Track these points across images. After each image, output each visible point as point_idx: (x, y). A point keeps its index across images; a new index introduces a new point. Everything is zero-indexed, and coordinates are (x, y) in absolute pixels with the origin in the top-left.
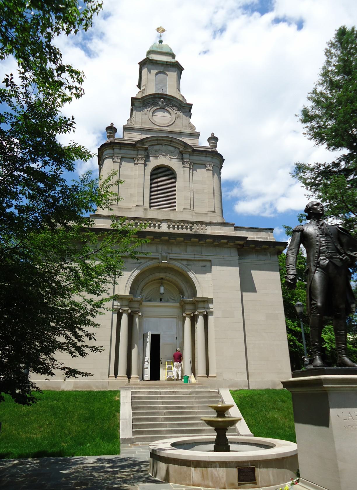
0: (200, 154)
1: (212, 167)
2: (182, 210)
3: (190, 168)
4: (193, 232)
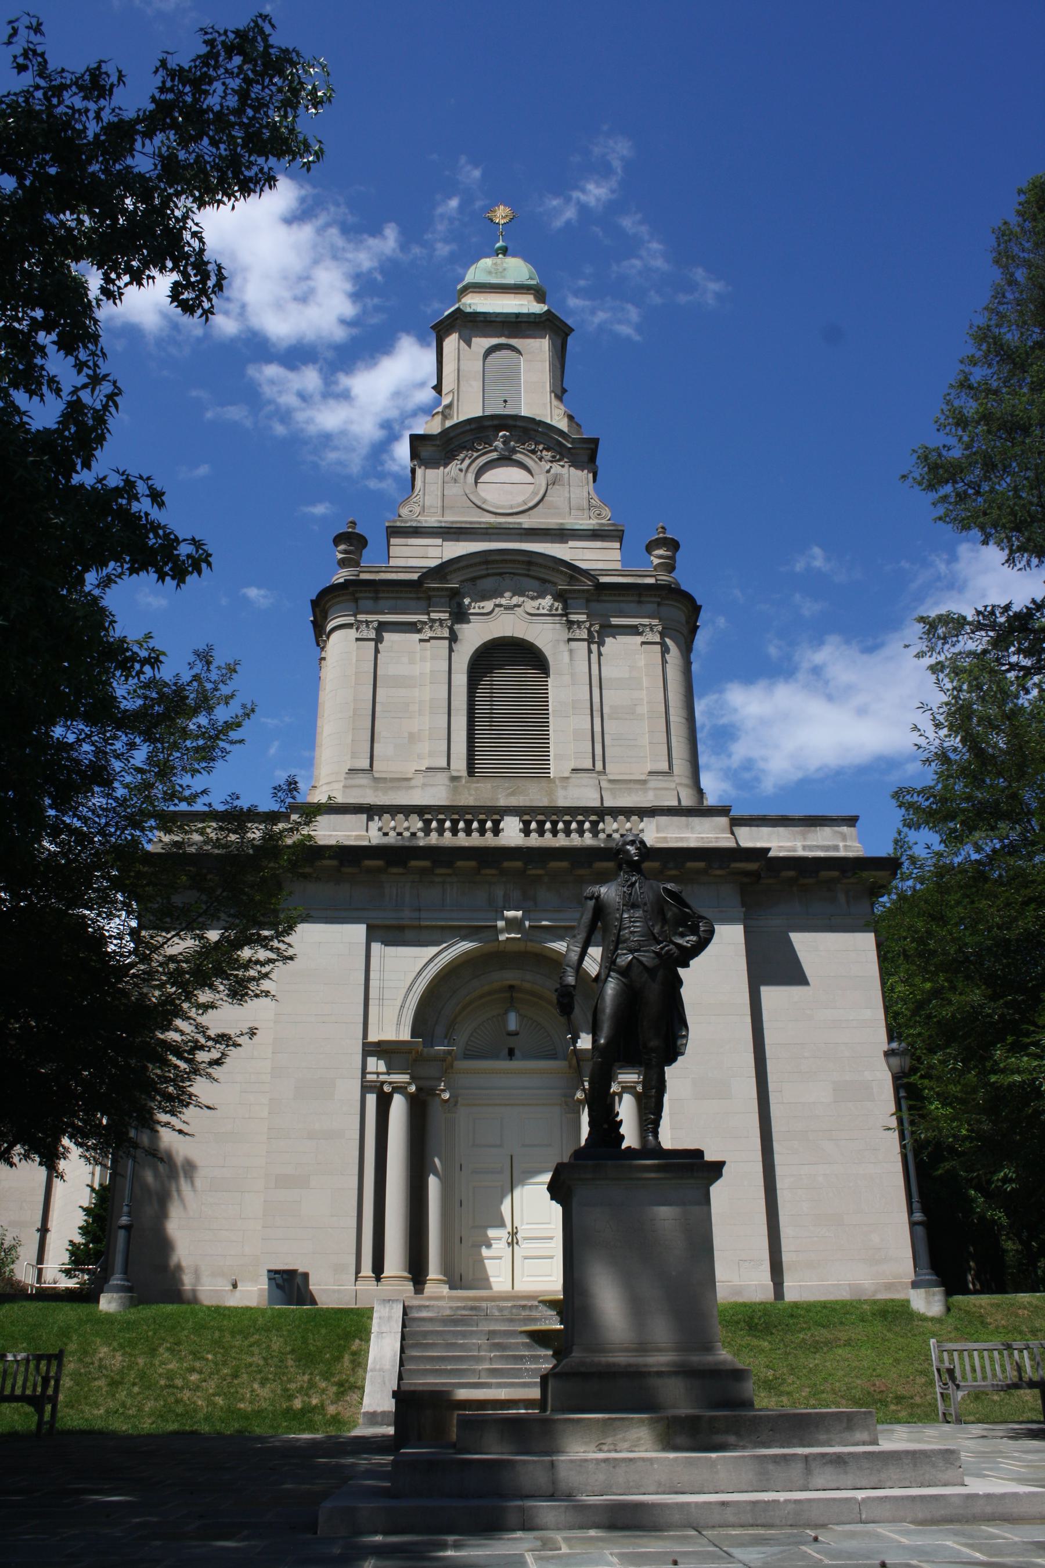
0: (619, 595)
1: (661, 633)
2: (567, 774)
3: (590, 641)
4: (600, 842)
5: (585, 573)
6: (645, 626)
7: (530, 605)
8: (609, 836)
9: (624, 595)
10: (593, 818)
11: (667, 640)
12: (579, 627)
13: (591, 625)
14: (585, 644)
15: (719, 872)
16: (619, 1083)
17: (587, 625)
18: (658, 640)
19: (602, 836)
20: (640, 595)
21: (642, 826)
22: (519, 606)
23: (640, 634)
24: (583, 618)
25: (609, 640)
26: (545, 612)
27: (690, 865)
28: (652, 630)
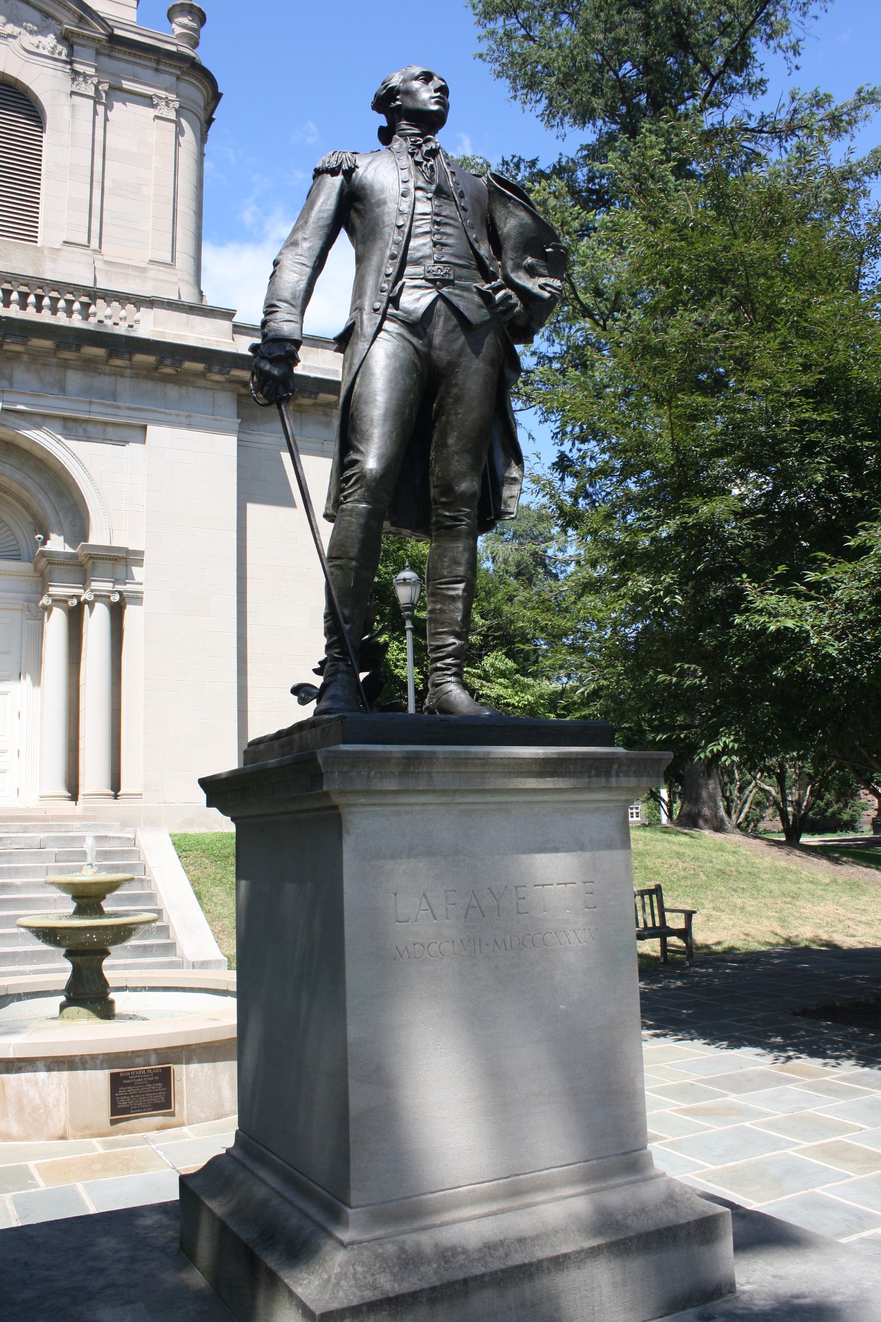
0: (135, 55)
1: (177, 111)
2: (58, 246)
3: (97, 101)
4: (91, 325)
5: (102, 21)
6: (161, 98)
7: (29, 40)
8: (101, 322)
9: (140, 57)
10: (85, 299)
11: (183, 121)
12: (85, 81)
13: (99, 83)
14: (92, 102)
15: (217, 377)
16: (92, 591)
17: (95, 80)
18: (173, 117)
19: (93, 320)
20: (158, 62)
21: (138, 316)
22: (15, 37)
23: (154, 106)
24: (91, 71)
25: (117, 105)
26: (46, 52)
27: (188, 365)
28: (167, 104)
